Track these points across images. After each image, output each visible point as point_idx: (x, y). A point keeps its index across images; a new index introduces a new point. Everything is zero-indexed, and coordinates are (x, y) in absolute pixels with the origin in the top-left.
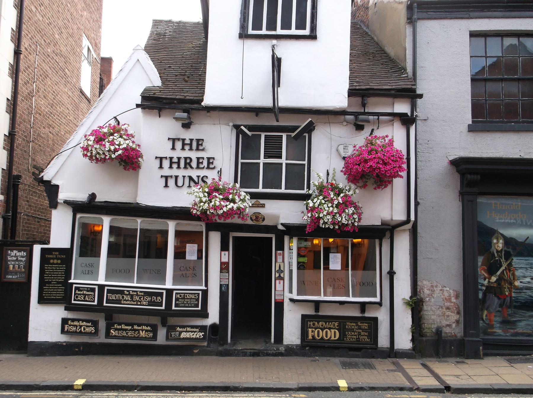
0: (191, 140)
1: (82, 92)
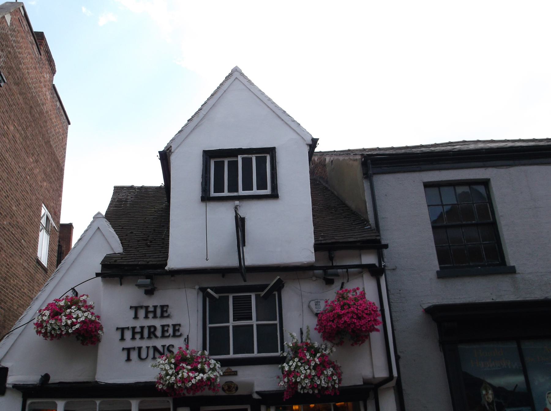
0: (155, 307)
1: (39, 262)
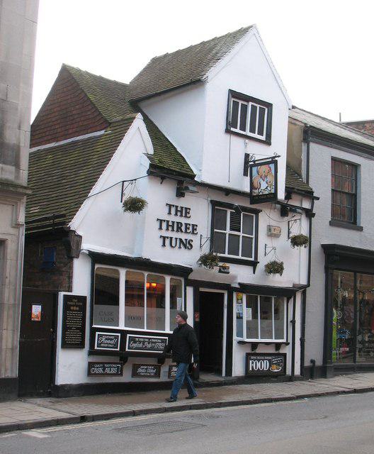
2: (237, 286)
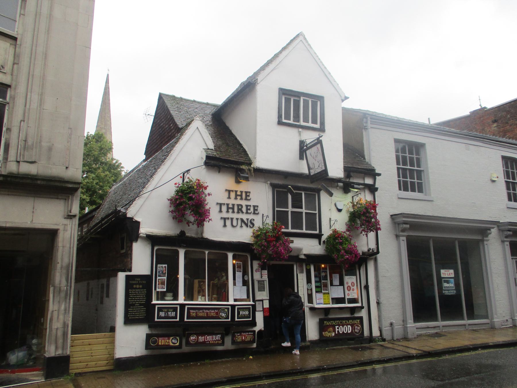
0: (242, 192)
2: (303, 257)
